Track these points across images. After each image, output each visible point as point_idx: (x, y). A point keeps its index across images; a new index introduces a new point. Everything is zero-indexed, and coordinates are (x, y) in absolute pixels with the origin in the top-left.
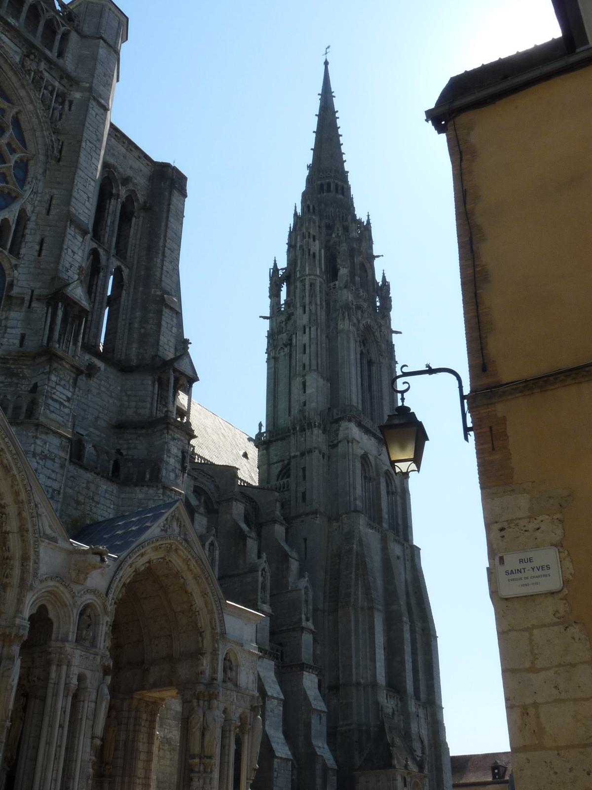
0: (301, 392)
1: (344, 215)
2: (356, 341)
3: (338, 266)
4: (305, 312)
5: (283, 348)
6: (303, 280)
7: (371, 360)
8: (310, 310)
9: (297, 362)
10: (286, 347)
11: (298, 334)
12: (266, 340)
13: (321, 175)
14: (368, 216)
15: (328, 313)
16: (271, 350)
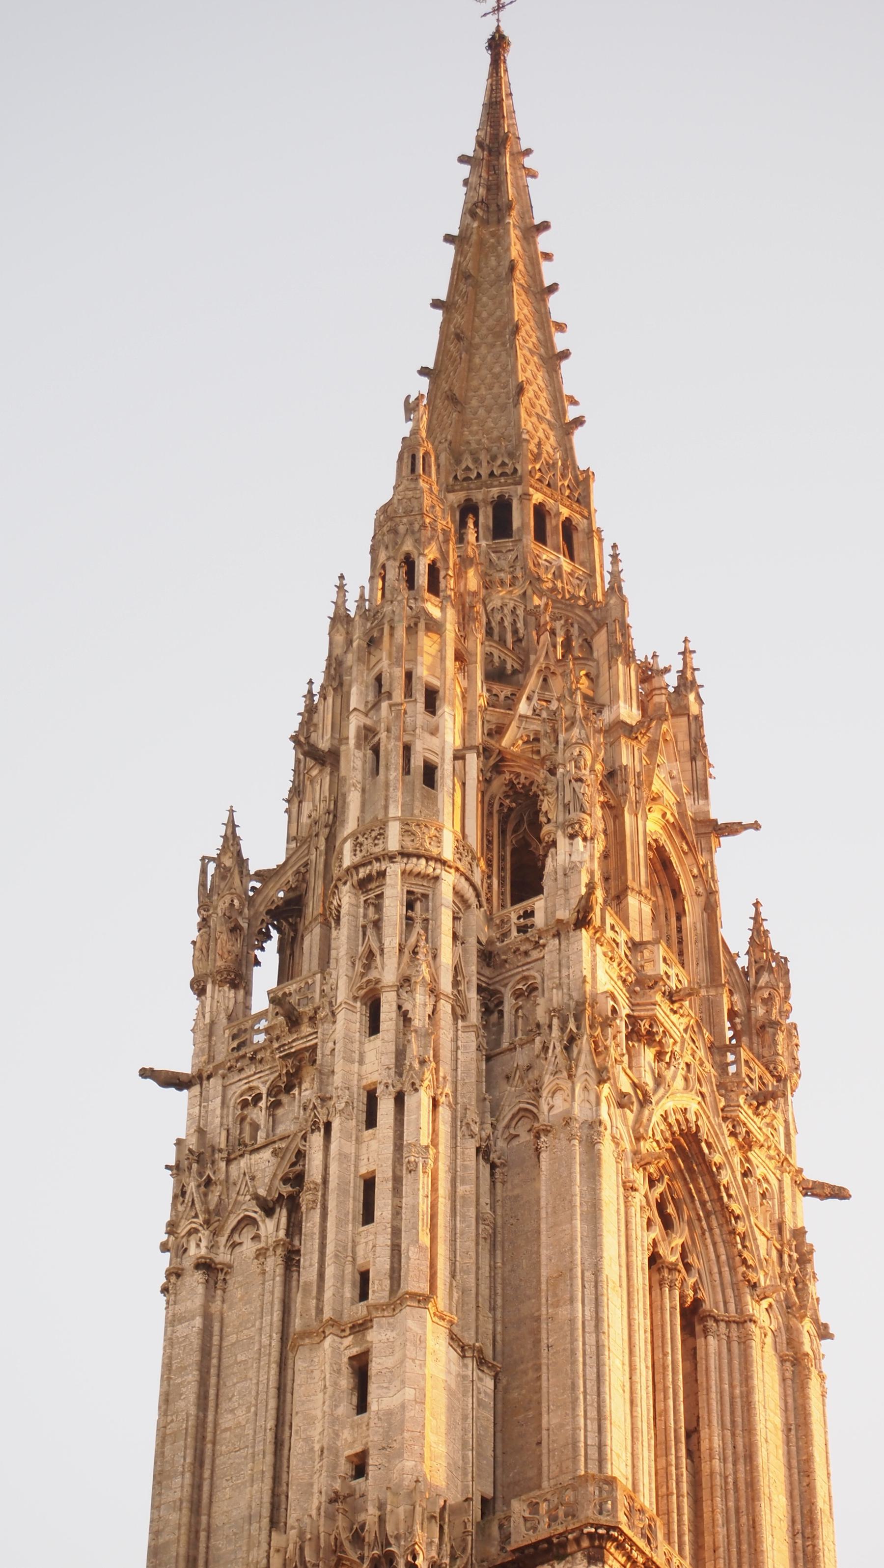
0: (346, 1407)
1: (575, 631)
2: (629, 1188)
3: (546, 829)
4: (374, 1028)
5: (252, 1222)
6: (369, 878)
7: (697, 1302)
8: (405, 1018)
9: (329, 1260)
10: (269, 1212)
11: (335, 1126)
12: (167, 1184)
13: (468, 469)
14: (686, 653)
15: (491, 1054)
16: (189, 1234)
